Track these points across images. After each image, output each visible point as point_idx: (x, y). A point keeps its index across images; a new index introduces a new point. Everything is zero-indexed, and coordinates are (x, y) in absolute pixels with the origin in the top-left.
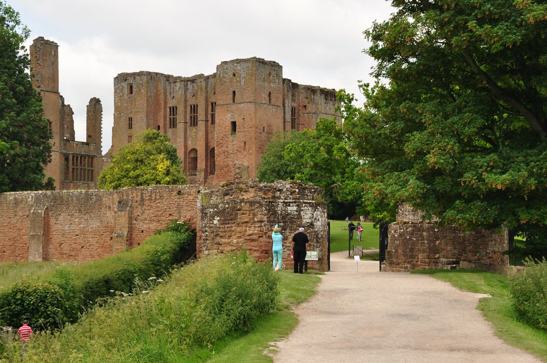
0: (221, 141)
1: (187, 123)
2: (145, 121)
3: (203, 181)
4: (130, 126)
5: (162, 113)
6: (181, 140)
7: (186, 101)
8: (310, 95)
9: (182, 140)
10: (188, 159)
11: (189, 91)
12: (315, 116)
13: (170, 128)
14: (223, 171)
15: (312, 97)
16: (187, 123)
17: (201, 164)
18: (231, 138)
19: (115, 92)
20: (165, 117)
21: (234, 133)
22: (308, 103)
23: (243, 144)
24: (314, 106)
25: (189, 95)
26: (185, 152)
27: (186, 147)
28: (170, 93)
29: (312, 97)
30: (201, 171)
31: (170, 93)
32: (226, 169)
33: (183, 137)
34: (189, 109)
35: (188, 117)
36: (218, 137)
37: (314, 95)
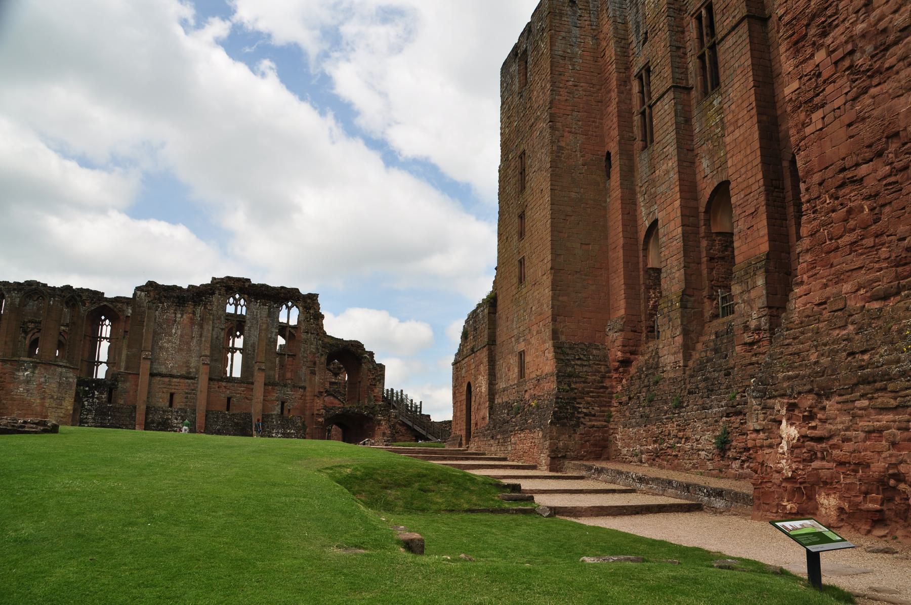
1: (688, 89)
4: (523, 188)
5: (613, 108)
6: (669, 167)
10: (704, 243)
13: (645, 147)
16: (688, 89)
17: (752, 239)
20: (624, 116)
27: (688, 188)
28: (638, 27)
31: (638, 27)
33: (672, 149)
34: (692, 32)
35: (693, 64)
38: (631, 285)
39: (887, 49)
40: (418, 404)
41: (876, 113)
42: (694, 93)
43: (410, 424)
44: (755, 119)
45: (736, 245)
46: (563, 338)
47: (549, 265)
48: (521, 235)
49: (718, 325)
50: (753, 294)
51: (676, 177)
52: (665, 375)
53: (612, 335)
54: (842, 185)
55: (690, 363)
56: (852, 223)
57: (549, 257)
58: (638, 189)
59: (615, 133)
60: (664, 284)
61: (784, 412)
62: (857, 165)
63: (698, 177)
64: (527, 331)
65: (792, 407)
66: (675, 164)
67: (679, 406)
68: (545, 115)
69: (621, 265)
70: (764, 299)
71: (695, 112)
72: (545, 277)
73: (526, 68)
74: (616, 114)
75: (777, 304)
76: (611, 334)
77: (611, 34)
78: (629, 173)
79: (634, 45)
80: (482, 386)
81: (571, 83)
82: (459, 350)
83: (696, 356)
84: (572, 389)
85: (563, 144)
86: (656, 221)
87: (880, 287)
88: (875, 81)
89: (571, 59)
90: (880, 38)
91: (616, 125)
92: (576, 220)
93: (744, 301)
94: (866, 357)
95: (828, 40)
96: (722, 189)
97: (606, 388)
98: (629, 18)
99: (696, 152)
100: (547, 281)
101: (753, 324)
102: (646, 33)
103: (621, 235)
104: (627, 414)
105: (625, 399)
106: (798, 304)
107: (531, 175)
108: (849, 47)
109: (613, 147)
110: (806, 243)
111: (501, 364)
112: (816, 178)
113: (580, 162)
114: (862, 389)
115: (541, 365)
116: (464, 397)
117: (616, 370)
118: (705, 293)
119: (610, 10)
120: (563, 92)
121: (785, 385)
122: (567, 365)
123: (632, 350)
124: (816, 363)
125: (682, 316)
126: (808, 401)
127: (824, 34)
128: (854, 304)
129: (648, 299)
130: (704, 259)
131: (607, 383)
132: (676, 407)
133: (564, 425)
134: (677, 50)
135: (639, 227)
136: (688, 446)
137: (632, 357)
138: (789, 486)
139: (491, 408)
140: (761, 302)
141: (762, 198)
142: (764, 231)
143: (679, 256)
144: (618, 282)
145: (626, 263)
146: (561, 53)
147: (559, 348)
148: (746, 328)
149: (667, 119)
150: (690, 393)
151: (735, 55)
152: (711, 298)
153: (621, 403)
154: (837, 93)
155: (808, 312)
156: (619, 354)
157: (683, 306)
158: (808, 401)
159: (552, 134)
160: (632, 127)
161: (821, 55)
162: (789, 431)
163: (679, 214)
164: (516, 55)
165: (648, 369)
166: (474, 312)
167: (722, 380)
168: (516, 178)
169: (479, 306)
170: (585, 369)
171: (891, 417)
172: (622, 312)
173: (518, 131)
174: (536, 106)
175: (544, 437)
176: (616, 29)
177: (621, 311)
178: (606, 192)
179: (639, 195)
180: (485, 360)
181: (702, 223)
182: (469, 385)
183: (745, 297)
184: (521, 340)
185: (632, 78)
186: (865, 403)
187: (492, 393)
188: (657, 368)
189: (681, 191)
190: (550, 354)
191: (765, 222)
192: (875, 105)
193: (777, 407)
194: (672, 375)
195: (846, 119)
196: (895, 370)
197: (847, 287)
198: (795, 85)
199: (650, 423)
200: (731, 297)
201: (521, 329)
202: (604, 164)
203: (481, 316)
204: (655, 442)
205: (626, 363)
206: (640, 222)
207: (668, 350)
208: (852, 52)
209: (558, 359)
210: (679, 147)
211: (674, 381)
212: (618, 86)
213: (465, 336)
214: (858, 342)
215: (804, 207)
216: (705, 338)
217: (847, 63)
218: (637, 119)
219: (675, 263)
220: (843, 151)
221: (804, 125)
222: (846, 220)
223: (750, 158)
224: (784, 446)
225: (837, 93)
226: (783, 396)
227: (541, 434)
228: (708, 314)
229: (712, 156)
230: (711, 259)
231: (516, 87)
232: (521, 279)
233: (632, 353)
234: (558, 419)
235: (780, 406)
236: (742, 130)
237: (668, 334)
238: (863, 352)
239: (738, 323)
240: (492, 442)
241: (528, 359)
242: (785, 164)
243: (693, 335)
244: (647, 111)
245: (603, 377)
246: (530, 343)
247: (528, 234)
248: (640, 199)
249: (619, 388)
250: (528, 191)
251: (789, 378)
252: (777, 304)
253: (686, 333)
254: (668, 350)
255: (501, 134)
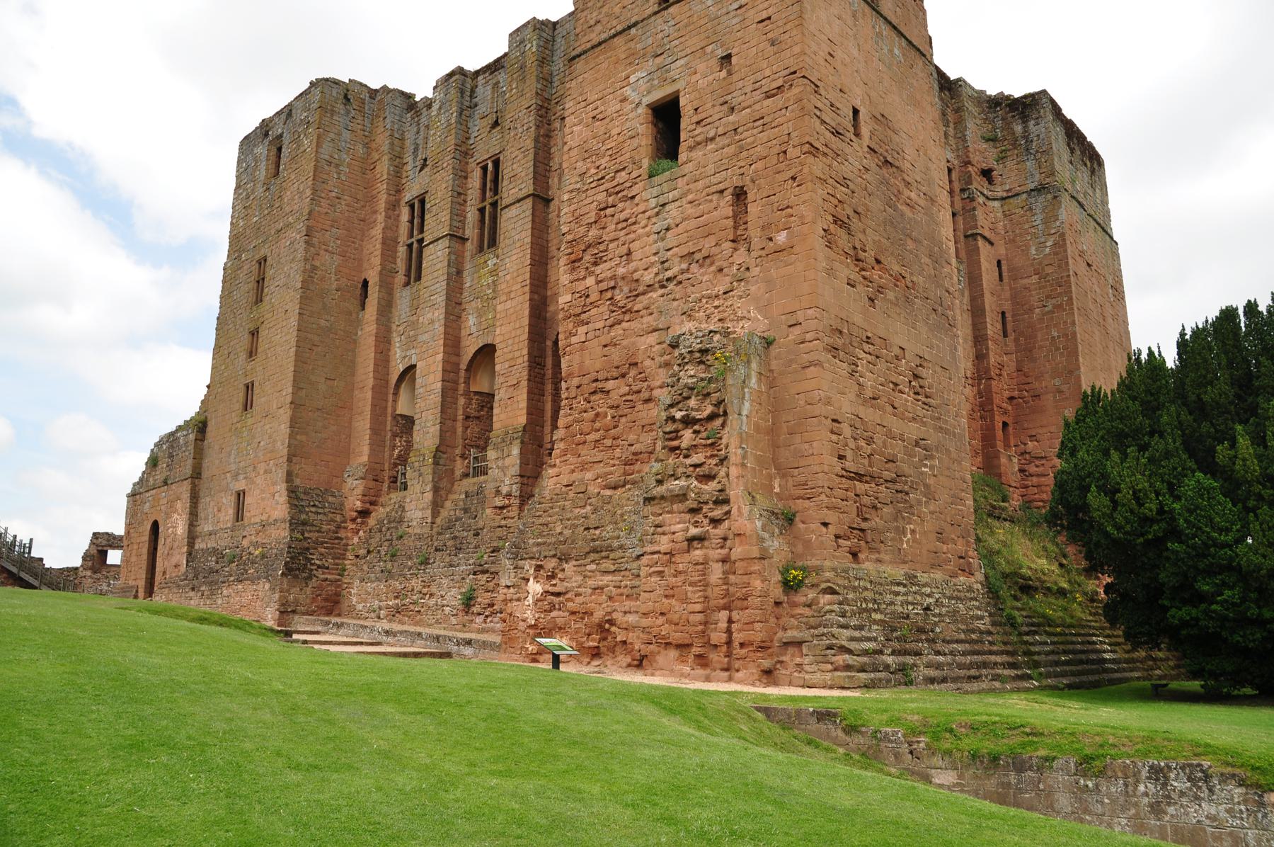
0: (593, 232)
1: (463, 240)
2: (300, 254)
3: (515, 490)
4: (259, 299)
5: (377, 232)
6: (434, 316)
7: (463, 151)
8: (1007, 127)
9: (439, 314)
10: (462, 401)
11: (482, 109)
12: (1041, 201)
13: (407, 284)
14: (600, 402)
15: (1018, 128)
16: (463, 240)
17: (511, 411)
18: (648, 195)
19: (238, 187)
20: (389, 245)
21: (665, 163)
22: (1001, 159)
23: (725, 206)
24: (1030, 164)
25: (478, 126)
26: (450, 370)
27: (453, 343)
28: (416, 149)
29: (1018, 128)
30: (506, 439)
31: (416, 149)
32: (618, 389)
33: (440, 299)
34: (475, 181)
35: (472, 215)
36: (577, 219)
37: (1025, 119)
38: (376, 431)
39: (637, 296)
40: (26, 541)
41: (625, 343)
42: (468, 244)
43: (14, 570)
44: (527, 296)
45: (495, 411)
46: (297, 482)
47: (289, 399)
48: (251, 354)
49: (470, 484)
50: (508, 461)
51: (442, 329)
52: (410, 530)
53: (351, 483)
54: (594, 393)
55: (438, 521)
56: (597, 425)
57: (290, 390)
58: (394, 327)
59: (377, 261)
60: (417, 437)
61: (532, 571)
62: (607, 379)
63: (463, 333)
64: (251, 468)
65: (539, 568)
66: (442, 316)
67: (426, 562)
68: (301, 226)
69: (368, 408)
70: (517, 467)
71: (468, 266)
72: (281, 411)
73: (279, 157)
74: (380, 240)
75: (531, 473)
76: (349, 480)
77: (385, 148)
78: (386, 308)
79: (409, 167)
80: (177, 526)
81: (334, 194)
82: (141, 479)
83: (444, 513)
84: (306, 539)
85: (317, 263)
86: (413, 367)
87: (613, 479)
88: (627, 317)
89: (337, 166)
90: (634, 285)
91: (378, 252)
92: (320, 349)
93: (498, 467)
94: (597, 532)
95: (598, 270)
96: (487, 352)
97: (341, 539)
98: (407, 135)
99: (463, 306)
100: (285, 415)
101: (505, 490)
102: (425, 160)
103: (371, 375)
104: (365, 567)
105: (362, 552)
106: (551, 481)
107: (270, 287)
108: (612, 284)
109: (373, 277)
110: (559, 434)
111: (207, 505)
112: (576, 381)
113: (334, 286)
114: (593, 556)
115: (268, 509)
116: (146, 538)
117: (353, 520)
118: (458, 451)
119: (388, 120)
120: (324, 203)
121: (535, 549)
122: (301, 512)
123: (372, 500)
124: (560, 533)
125: (434, 473)
126: (551, 564)
127: (596, 264)
128: (593, 489)
129: (394, 447)
130: (460, 417)
131: (342, 534)
132: (421, 564)
133: (296, 577)
134: (459, 196)
135: (391, 370)
136: (432, 602)
137: (372, 508)
138: (531, 632)
139: (189, 554)
140: (515, 470)
141: (525, 373)
142: (524, 404)
143: (435, 411)
144: (363, 425)
145: (374, 406)
146: (327, 157)
147: (292, 492)
148: (498, 492)
149: (439, 266)
150: (437, 550)
151: (516, 225)
152: (463, 457)
153: (357, 556)
154: (600, 315)
155: (557, 491)
156: (358, 504)
157: (436, 463)
158: (551, 564)
159: (305, 250)
160: (395, 258)
161: (590, 281)
162: (535, 588)
163: (440, 368)
164: (266, 135)
165: (389, 522)
166: (172, 434)
167: (471, 539)
168: (251, 286)
169: (180, 428)
170: (320, 517)
171: (610, 578)
172: (365, 459)
173: (258, 228)
174: (287, 209)
175: (272, 589)
176: (392, 144)
177: (363, 455)
178: (358, 323)
179: (394, 335)
180: (186, 496)
181: (462, 380)
182: (155, 525)
183: (500, 463)
184: (241, 477)
185: (403, 203)
186: (593, 567)
187: (192, 538)
188: (401, 521)
189: (445, 345)
190: (282, 497)
191: (525, 396)
192: (625, 337)
193: (527, 567)
194: (418, 531)
195: (604, 339)
196: (616, 544)
197: (589, 475)
198: (568, 298)
199: (392, 578)
200: (484, 459)
201: (242, 464)
202: (358, 292)
203: (182, 441)
204: (396, 597)
205: (364, 513)
206: (392, 364)
207: (415, 504)
208: (613, 288)
209: (292, 506)
210: (448, 299)
211: (420, 537)
212: (387, 210)
213: (153, 462)
214: (593, 521)
215: (563, 403)
216: (452, 497)
217: (609, 295)
218: (402, 250)
219: (431, 417)
220: (598, 366)
221: (571, 335)
222: (593, 421)
223: (518, 332)
224: (530, 600)
225: (600, 315)
226: (532, 558)
227: (267, 586)
228: (458, 473)
229: (480, 316)
230: (467, 418)
231: (262, 173)
232: (247, 406)
233: (372, 503)
234: (289, 570)
235: (529, 566)
236: (514, 302)
237: (418, 488)
238: (596, 528)
239: (490, 487)
240: (192, 594)
241: (248, 500)
242: (549, 343)
243: (443, 493)
244: (415, 245)
245: (339, 527)
246: (253, 482)
247: (260, 356)
248: (396, 339)
249: (356, 540)
250: (265, 306)
251: (538, 544)
252: (531, 473)
253: (436, 490)
254: (415, 504)
255: (232, 224)
